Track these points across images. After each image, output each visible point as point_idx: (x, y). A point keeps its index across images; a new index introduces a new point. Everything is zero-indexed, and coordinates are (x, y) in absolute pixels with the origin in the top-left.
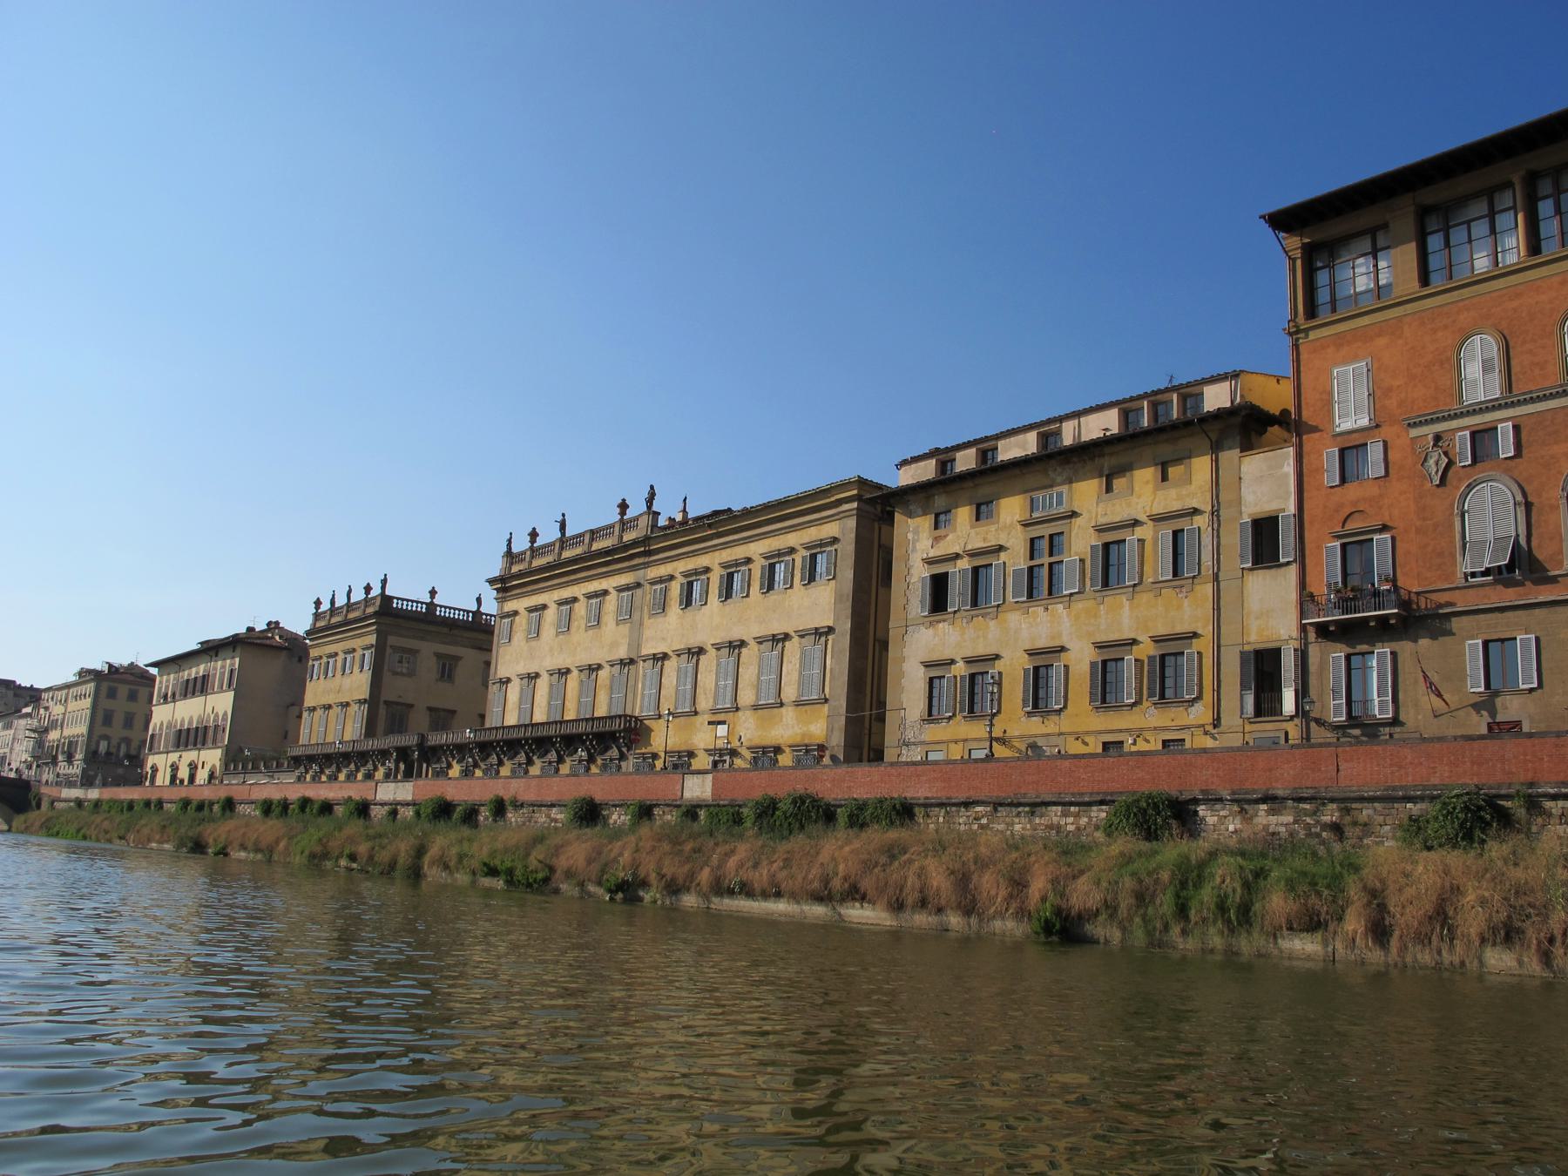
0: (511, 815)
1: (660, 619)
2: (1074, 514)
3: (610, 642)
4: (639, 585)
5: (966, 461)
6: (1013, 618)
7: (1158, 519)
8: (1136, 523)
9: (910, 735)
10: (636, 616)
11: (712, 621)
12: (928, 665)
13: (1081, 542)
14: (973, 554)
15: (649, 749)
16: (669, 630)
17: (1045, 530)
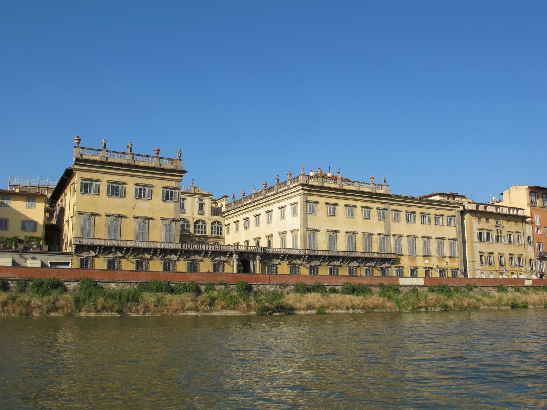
0: (474, 289)
1: (397, 223)
2: (503, 227)
3: (376, 227)
4: (387, 210)
5: (481, 208)
6: (495, 245)
7: (516, 232)
8: (513, 232)
9: (477, 268)
10: (386, 220)
11: (418, 229)
12: (480, 253)
13: (505, 234)
14: (487, 230)
15: (400, 265)
16: (401, 227)
17: (499, 229)
